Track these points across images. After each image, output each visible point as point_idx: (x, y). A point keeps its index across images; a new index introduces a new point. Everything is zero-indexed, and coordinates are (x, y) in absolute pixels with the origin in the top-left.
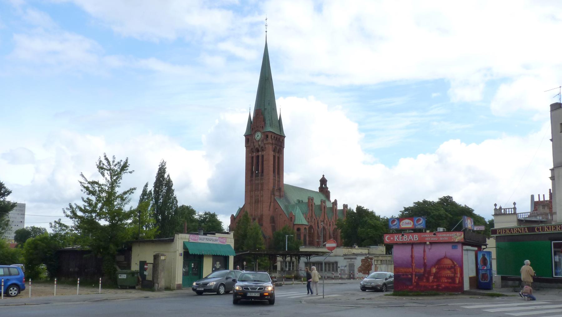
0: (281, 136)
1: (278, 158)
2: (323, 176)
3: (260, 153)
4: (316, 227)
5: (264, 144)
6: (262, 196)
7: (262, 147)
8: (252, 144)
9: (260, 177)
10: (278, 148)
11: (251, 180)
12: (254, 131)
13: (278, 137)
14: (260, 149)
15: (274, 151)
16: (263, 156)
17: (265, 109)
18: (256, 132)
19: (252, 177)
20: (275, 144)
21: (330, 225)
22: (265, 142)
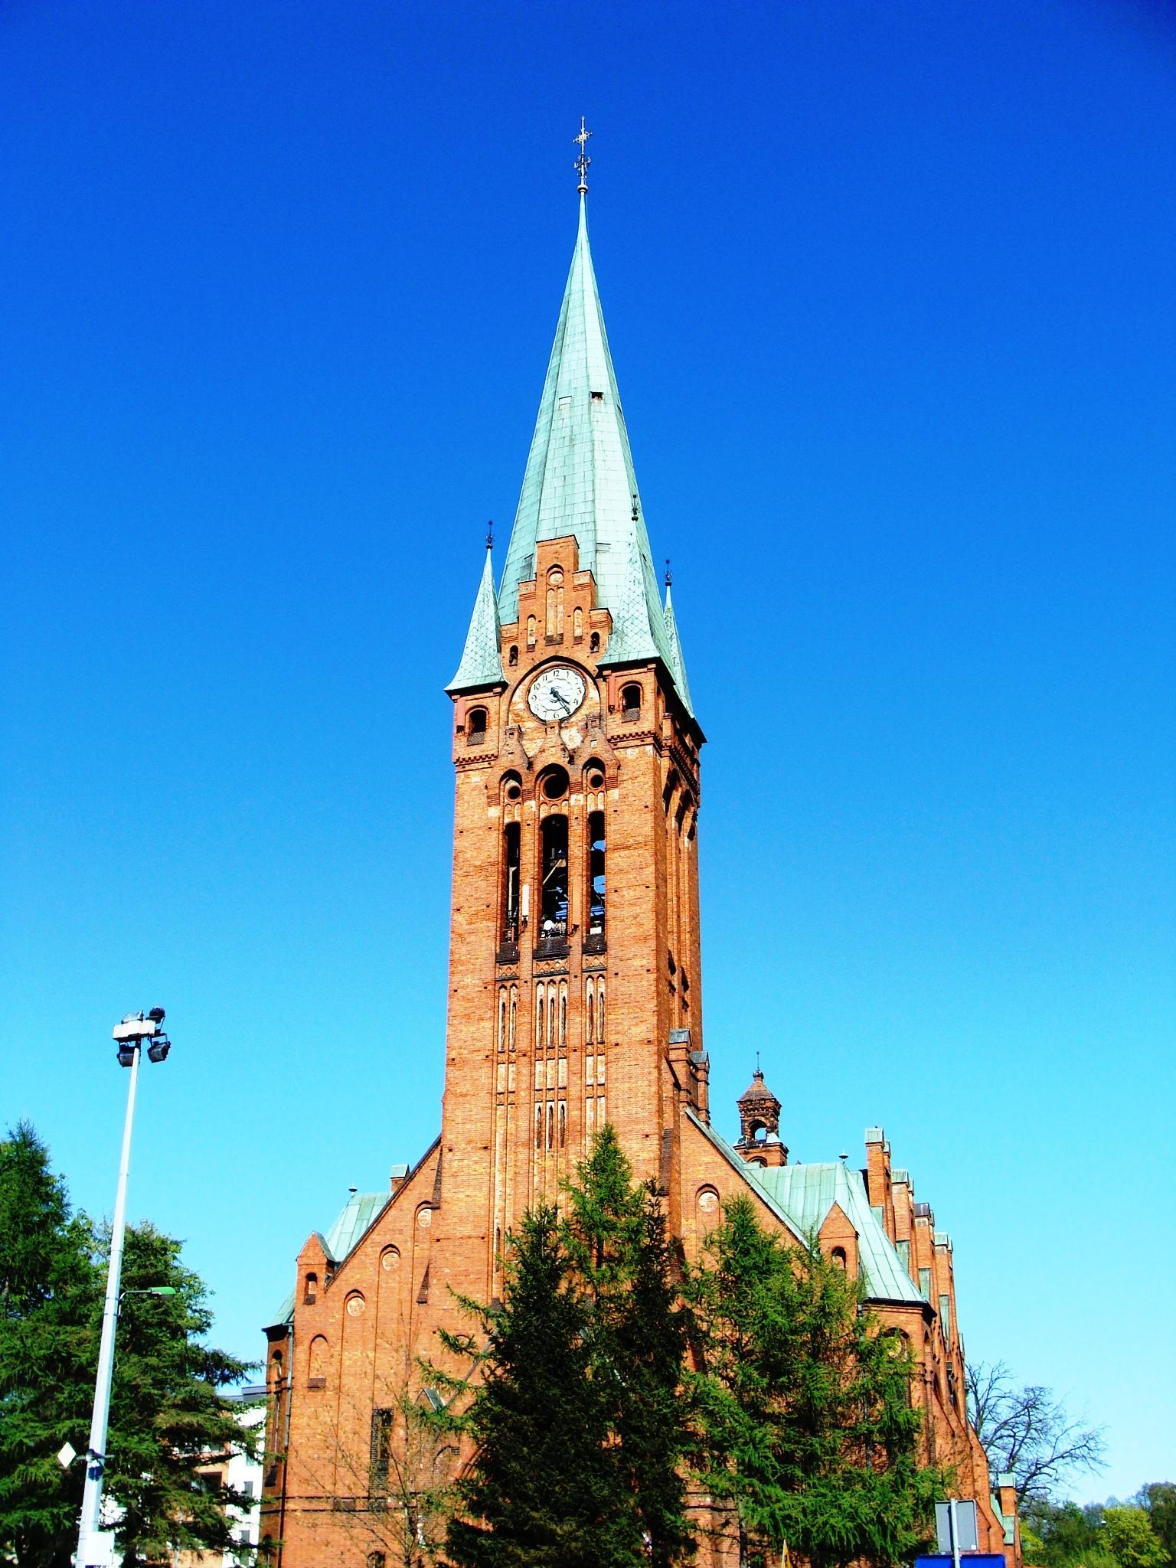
5: (613, 741)
7: (594, 762)
8: (513, 741)
12: (525, 662)
14: (575, 773)
16: (597, 823)
17: (598, 547)
19: (507, 955)
22: (616, 725)
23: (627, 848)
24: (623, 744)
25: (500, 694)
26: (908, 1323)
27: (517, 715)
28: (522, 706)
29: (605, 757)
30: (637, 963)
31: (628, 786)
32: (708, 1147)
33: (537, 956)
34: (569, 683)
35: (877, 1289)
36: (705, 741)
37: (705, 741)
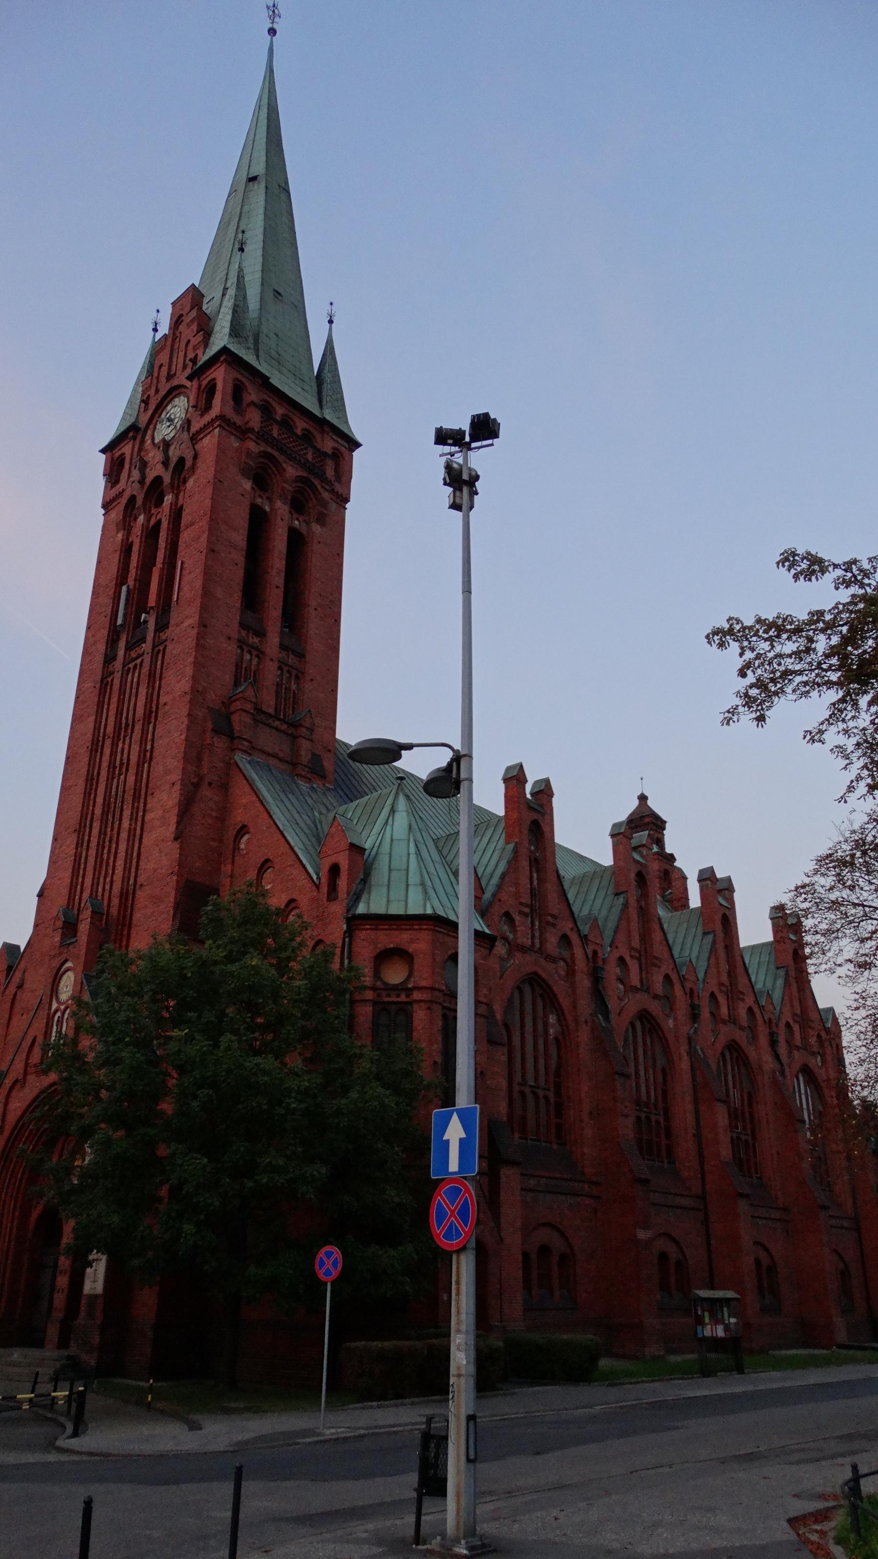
0: (323, 424)
1: (297, 543)
2: (643, 798)
3: (168, 499)
4: (585, 1006)
6: (146, 757)
7: (181, 461)
9: (147, 646)
10: (291, 471)
11: (104, 685)
13: (301, 425)
14: (167, 479)
15: (261, 480)
18: (161, 407)
20: (263, 436)
21: (695, 1016)
23: (192, 524)
24: (202, 436)
25: (134, 438)
26: (412, 941)
27: (146, 451)
28: (149, 442)
29: (189, 455)
30: (186, 624)
31: (199, 472)
32: (247, 789)
33: (129, 648)
34: (178, 408)
35: (375, 903)
36: (358, 445)
37: (358, 445)
